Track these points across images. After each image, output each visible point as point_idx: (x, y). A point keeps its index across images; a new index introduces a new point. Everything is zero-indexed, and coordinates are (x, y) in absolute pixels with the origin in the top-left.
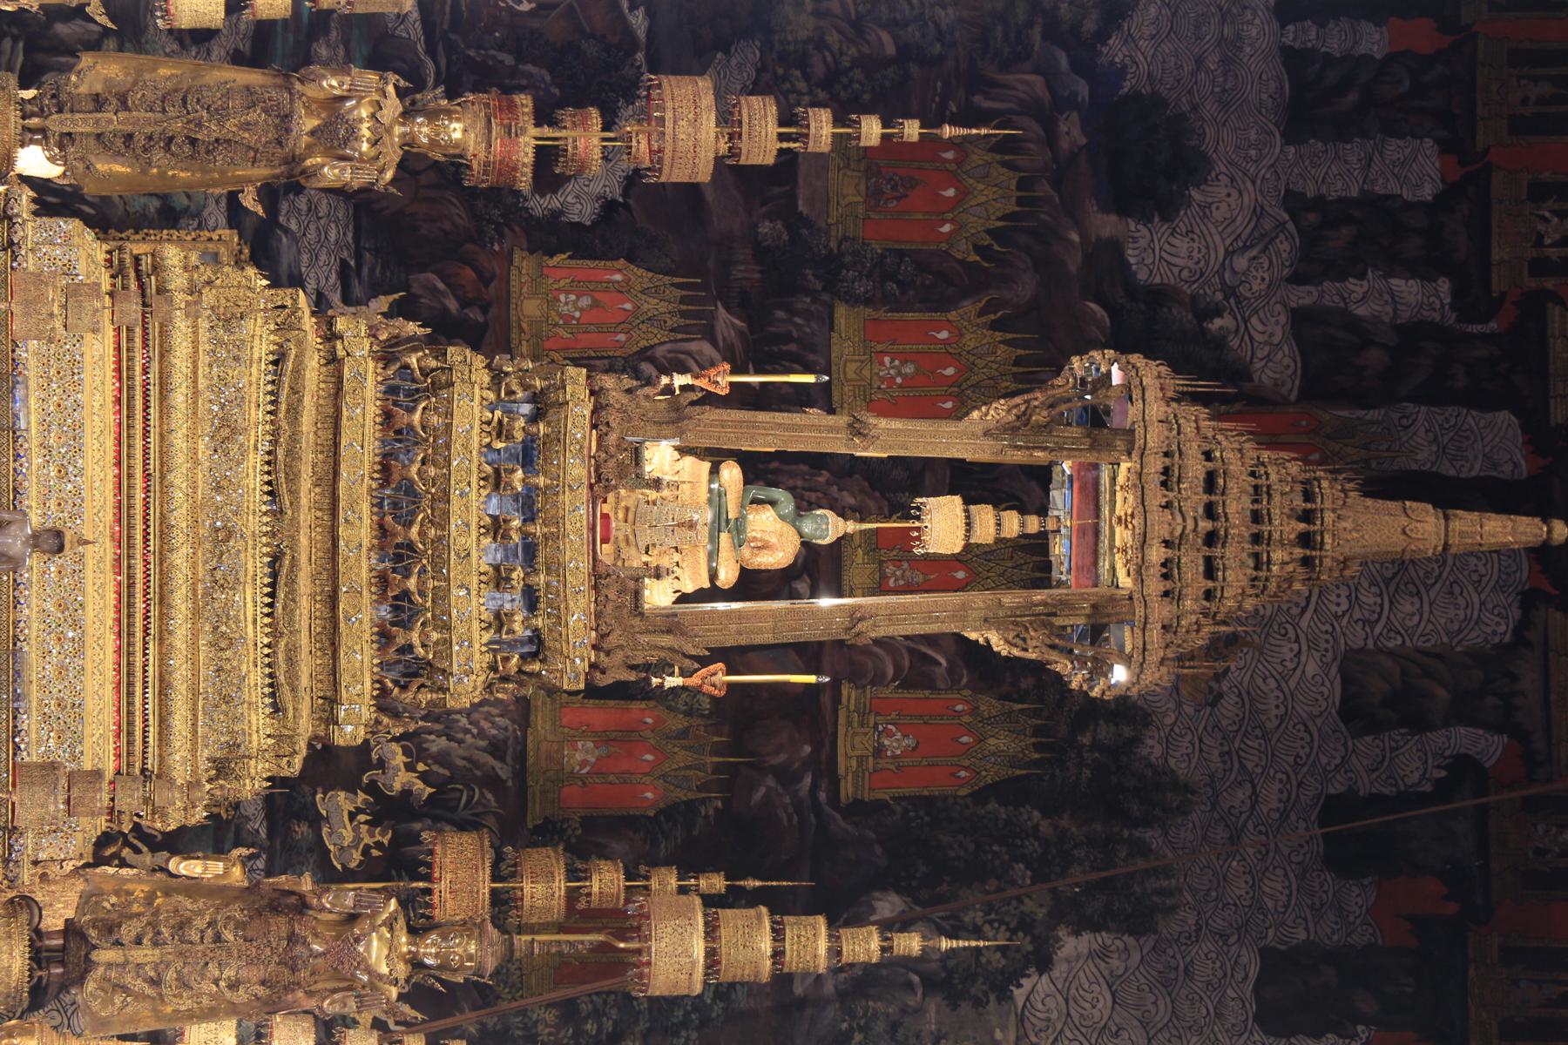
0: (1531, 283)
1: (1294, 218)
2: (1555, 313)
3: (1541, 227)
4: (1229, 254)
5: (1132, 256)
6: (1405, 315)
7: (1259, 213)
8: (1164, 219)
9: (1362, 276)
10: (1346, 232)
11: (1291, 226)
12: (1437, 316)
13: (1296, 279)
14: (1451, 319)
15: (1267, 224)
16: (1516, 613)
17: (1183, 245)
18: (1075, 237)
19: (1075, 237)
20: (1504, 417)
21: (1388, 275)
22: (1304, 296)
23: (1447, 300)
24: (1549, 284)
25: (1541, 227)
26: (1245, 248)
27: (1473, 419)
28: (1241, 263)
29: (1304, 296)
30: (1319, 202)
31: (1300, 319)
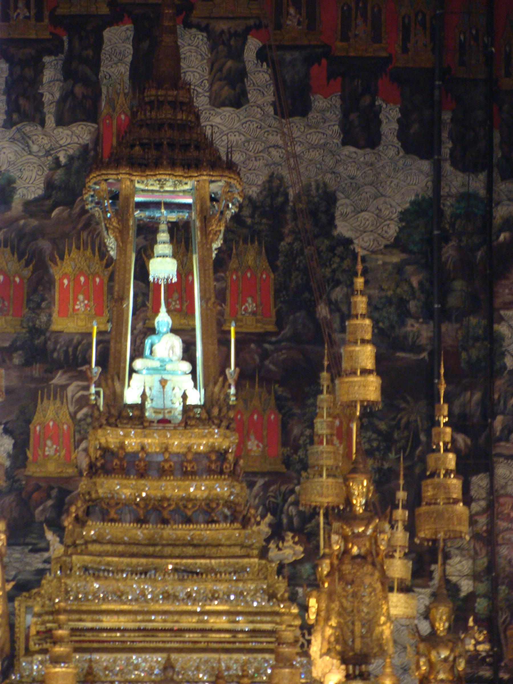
0: (46, 21)
1: (15, 124)
2: (60, 11)
3: (21, 17)
4: (30, 153)
5: (31, 197)
6: (61, 77)
7: (13, 140)
8: (14, 182)
9: (42, 95)
10: (22, 101)
11: (19, 126)
12: (60, 62)
13: (42, 123)
14: (62, 56)
15: (18, 136)
16: (194, 31)
17: (26, 174)
18: (22, 222)
19: (22, 222)
20: (106, 34)
21: (41, 83)
22: (50, 120)
23: (53, 58)
24: (46, 13)
25: (21, 17)
26: (28, 146)
27: (107, 47)
28: (35, 148)
29: (50, 120)
30: (9, 113)
31: (60, 122)
